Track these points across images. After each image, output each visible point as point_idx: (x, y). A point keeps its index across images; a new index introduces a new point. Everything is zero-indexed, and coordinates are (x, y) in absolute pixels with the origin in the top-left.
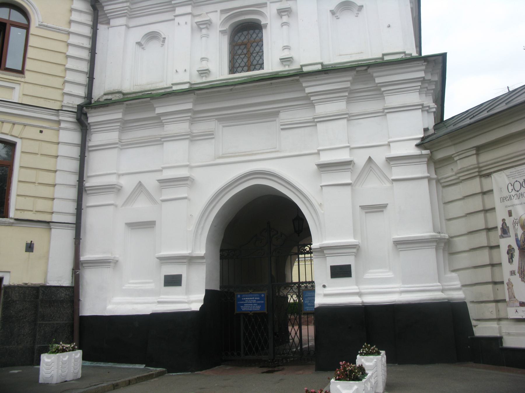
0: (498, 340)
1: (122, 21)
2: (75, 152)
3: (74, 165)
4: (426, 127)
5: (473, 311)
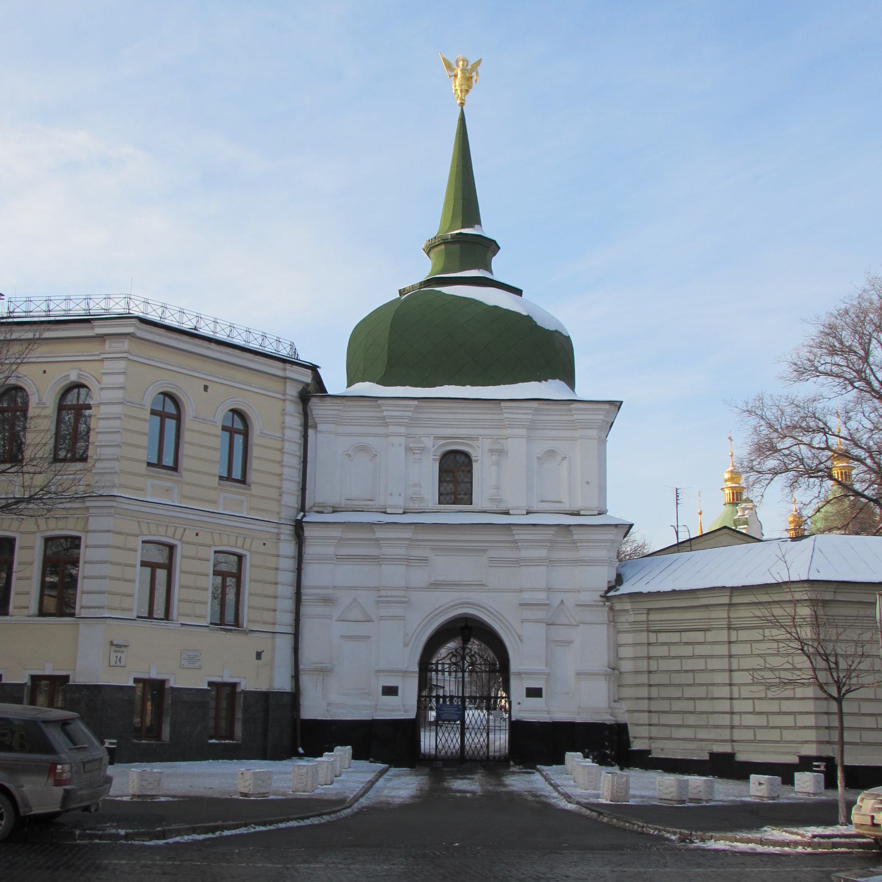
0: (649, 752)
1: (331, 427)
2: (291, 564)
3: (290, 577)
4: (609, 580)
5: (632, 731)
